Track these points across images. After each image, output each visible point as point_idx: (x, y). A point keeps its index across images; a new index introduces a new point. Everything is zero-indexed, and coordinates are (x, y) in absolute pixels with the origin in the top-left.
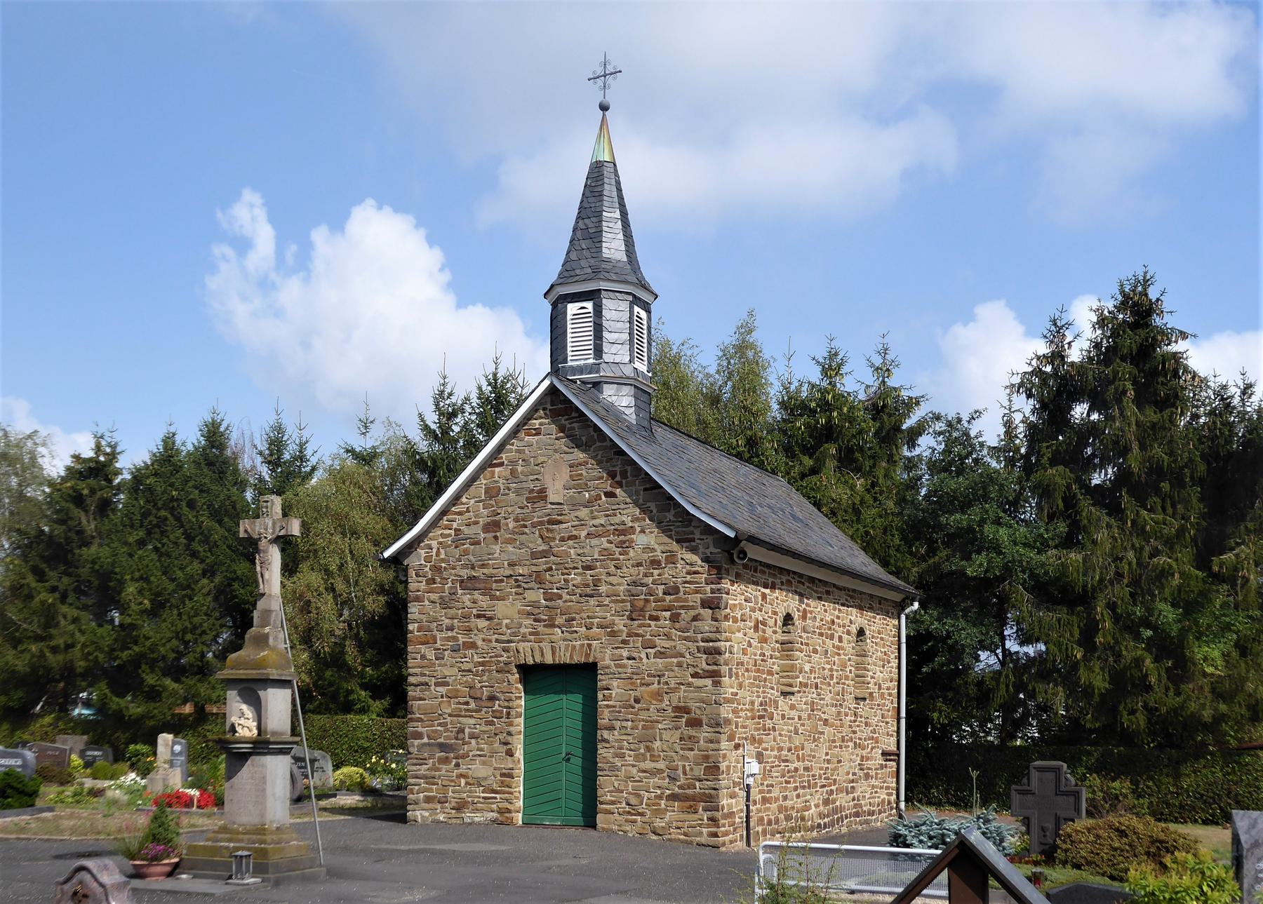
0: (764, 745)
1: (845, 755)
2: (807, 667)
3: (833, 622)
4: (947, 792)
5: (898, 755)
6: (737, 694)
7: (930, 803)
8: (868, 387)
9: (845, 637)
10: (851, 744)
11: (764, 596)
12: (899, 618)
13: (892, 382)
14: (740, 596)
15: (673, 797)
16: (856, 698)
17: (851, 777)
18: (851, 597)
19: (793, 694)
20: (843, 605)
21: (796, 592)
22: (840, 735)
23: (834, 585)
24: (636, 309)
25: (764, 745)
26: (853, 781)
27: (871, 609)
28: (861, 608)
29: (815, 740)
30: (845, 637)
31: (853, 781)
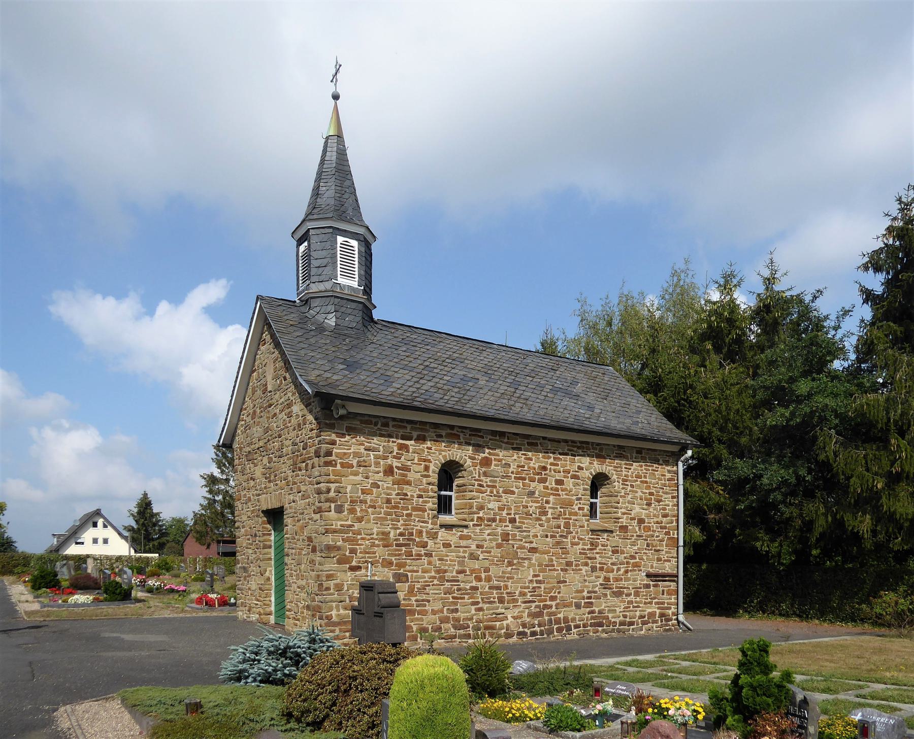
0: (408, 568)
1: (570, 576)
2: (493, 505)
3: (545, 468)
4: (792, 605)
5: (677, 576)
6: (351, 526)
7: (781, 615)
8: (759, 295)
9: (569, 483)
10: (584, 568)
11: (402, 447)
12: (677, 465)
13: (777, 287)
14: (350, 446)
15: (308, 607)
16: (592, 531)
17: (585, 594)
18: (579, 448)
19: (466, 527)
20: (560, 454)
21: (469, 444)
22: (563, 561)
23: (544, 438)
24: (340, 239)
25: (408, 568)
26: (590, 598)
27: (620, 456)
28: (599, 456)
29: (510, 564)
30: (569, 483)
31: (590, 598)
